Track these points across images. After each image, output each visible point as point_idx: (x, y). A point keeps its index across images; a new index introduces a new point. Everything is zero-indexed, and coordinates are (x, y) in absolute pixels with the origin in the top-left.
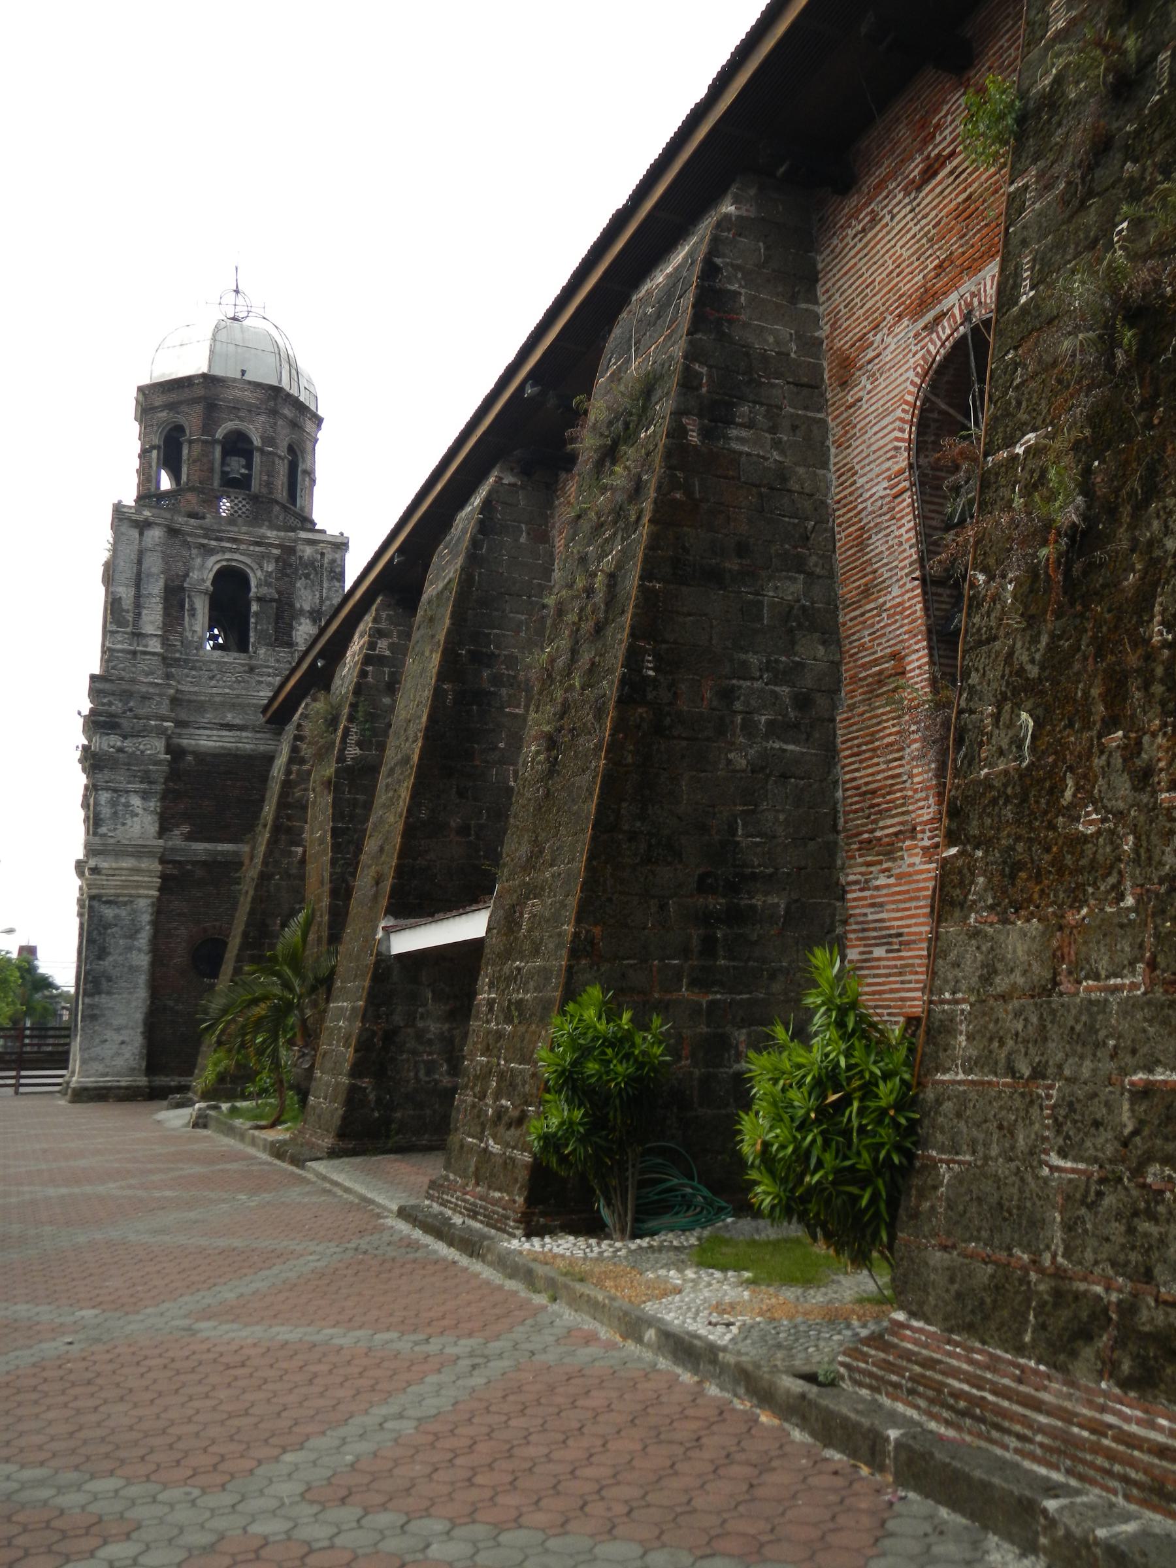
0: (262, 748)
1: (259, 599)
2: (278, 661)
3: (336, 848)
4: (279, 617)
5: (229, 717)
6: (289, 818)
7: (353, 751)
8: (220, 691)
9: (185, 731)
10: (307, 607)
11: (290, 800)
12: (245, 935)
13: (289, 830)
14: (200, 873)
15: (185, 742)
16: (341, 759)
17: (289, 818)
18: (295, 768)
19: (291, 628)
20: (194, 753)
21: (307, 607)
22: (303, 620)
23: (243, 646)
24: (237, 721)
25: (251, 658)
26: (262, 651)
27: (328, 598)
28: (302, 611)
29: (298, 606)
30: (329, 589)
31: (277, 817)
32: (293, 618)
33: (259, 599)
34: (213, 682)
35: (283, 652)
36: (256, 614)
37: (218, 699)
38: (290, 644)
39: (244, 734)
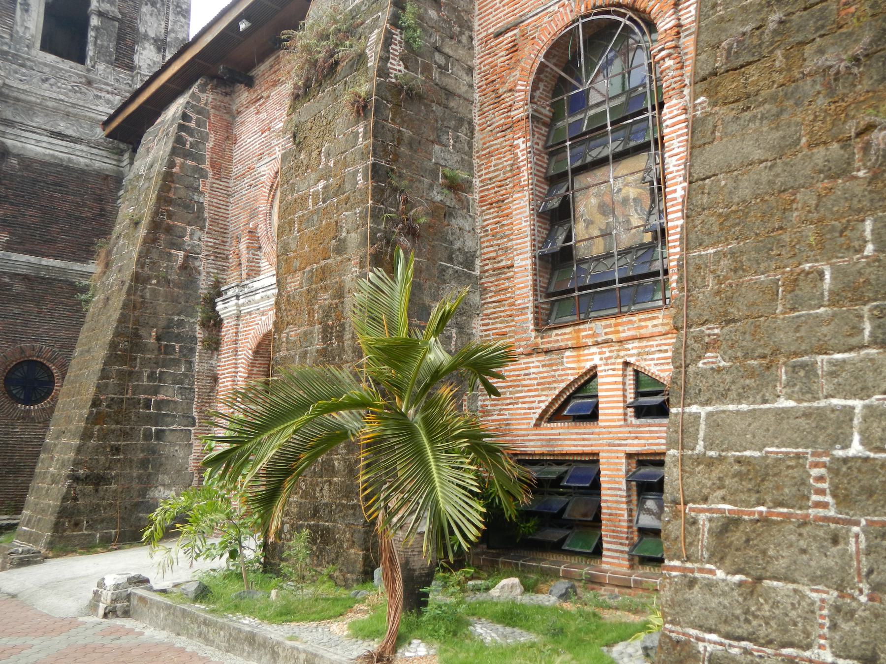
0: (97, 165)
1: (101, 14)
2: (117, 81)
3: (378, 194)
4: (120, 38)
5: (62, 126)
6: (170, 216)
7: (397, 67)
8: (54, 95)
9: (9, 130)
10: (152, 34)
11: (171, 195)
12: (113, 345)
13: (169, 230)
14: (19, 287)
15: (9, 142)
16: (383, 72)
17: (170, 216)
18: (179, 161)
19: (133, 51)
20: (18, 156)
21: (152, 34)
22: (147, 45)
23: (81, 59)
24: (70, 132)
25: (89, 70)
26: (101, 67)
27: (173, 31)
28: (146, 37)
29: (142, 30)
30: (175, 22)
31: (156, 213)
32: (135, 42)
33: (101, 14)
34: (46, 85)
35: (123, 74)
36: (97, 29)
37: (50, 104)
38: (131, 67)
39: (78, 146)
